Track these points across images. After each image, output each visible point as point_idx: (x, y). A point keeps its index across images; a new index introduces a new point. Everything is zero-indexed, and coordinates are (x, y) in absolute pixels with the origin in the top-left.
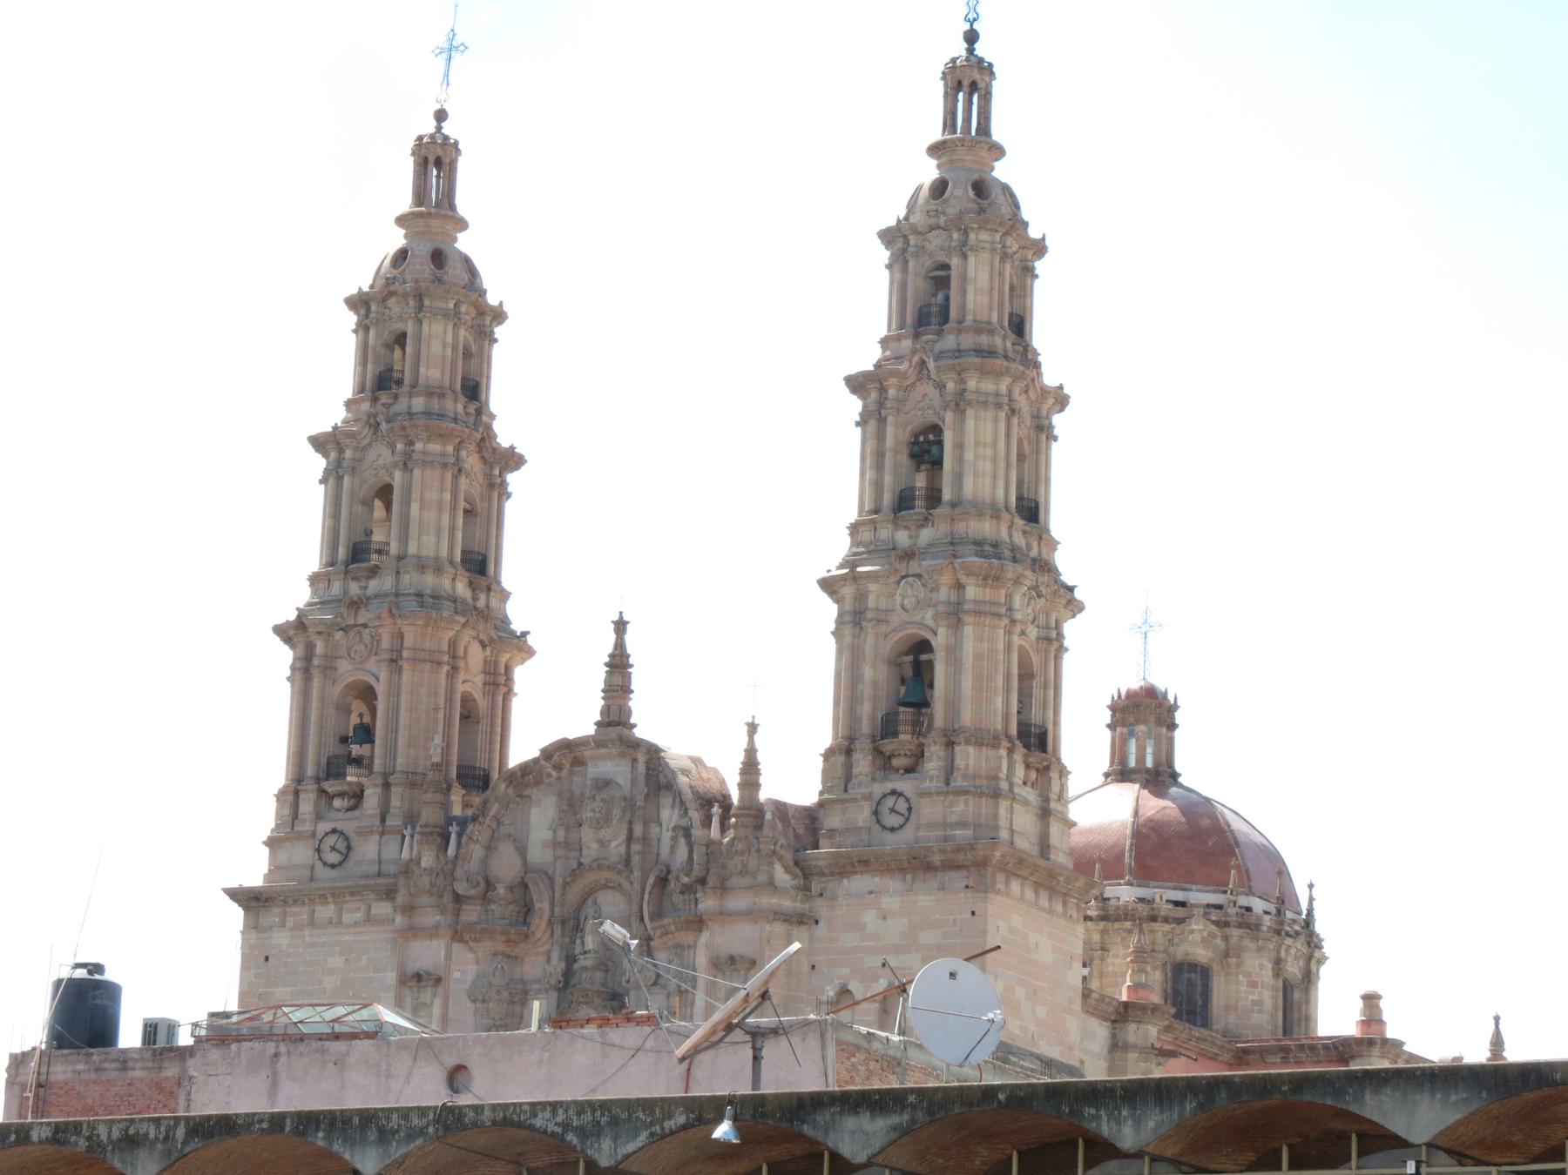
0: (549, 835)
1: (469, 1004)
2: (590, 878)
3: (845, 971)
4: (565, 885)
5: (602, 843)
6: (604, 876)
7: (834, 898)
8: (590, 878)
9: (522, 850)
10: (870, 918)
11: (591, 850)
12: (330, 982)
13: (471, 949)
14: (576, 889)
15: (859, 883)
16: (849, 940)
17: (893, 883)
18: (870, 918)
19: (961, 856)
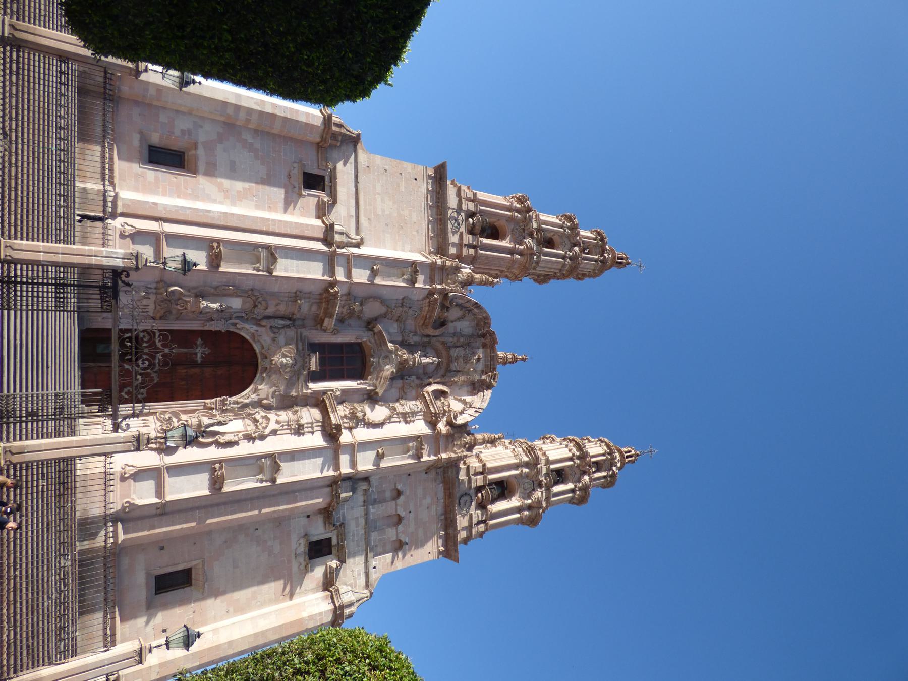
0: (458, 330)
1: (401, 297)
2: (444, 353)
3: (408, 493)
4: (443, 343)
5: (457, 358)
6: (445, 361)
7: (435, 480)
8: (444, 353)
9: (459, 319)
10: (428, 501)
11: (454, 353)
12: (406, 213)
13: (424, 299)
14: (440, 347)
15: (441, 494)
16: (420, 492)
17: (441, 509)
18: (428, 501)
19: (452, 544)
